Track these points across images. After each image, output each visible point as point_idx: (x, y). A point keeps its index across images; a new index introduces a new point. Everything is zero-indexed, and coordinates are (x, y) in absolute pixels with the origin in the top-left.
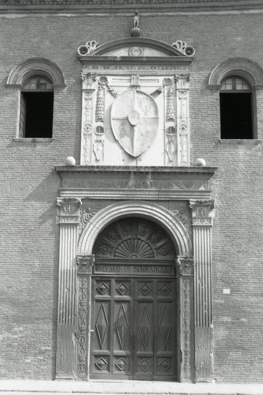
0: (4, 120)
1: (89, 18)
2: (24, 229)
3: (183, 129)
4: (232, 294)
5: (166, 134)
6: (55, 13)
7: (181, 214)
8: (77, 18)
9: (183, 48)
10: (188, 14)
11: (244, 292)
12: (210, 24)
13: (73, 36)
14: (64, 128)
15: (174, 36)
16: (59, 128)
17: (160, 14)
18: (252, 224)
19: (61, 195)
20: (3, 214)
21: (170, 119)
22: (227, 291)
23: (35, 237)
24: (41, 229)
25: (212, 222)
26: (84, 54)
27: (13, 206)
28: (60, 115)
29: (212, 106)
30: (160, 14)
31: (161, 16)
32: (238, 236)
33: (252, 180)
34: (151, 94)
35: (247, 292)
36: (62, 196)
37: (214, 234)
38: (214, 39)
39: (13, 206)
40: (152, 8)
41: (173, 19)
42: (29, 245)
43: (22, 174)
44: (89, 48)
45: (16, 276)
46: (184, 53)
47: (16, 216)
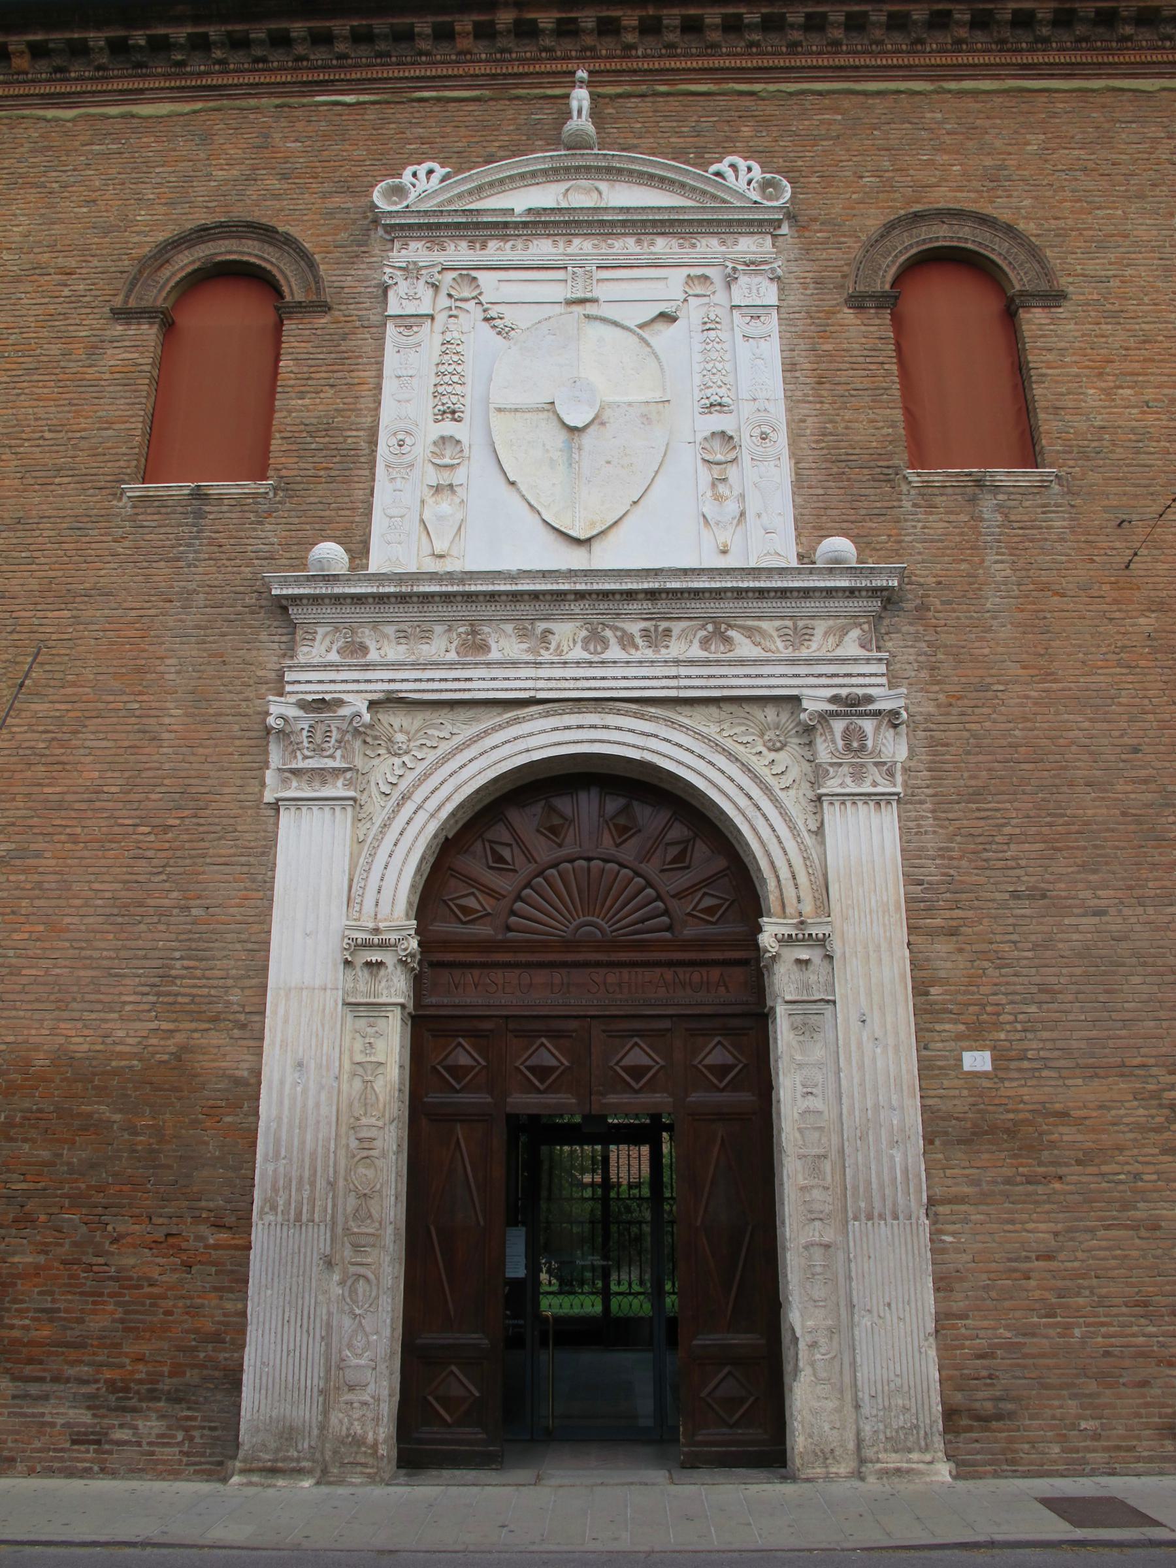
0: (97, 426)
1: (422, 104)
2: (137, 821)
3: (764, 437)
4: (1001, 1074)
5: (699, 457)
6: (303, 94)
7: (770, 750)
8: (377, 106)
9: (749, 183)
10: (757, 87)
11: (1051, 1064)
12: (839, 117)
13: (362, 158)
14: (313, 446)
15: (717, 150)
16: (294, 447)
17: (663, 88)
18: (1057, 781)
19: (288, 688)
20: (59, 767)
21: (712, 405)
22: (977, 1061)
23: (179, 853)
24: (202, 821)
25: (899, 779)
26: (395, 204)
27: (102, 736)
28: (300, 402)
29: (868, 360)
30: (663, 88)
31: (668, 94)
32: (1007, 830)
33: (1041, 615)
34: (641, 326)
35: (1062, 1063)
36: (289, 693)
37: (911, 824)
38: (855, 159)
39: (102, 736)
40: (635, 72)
41: (712, 104)
42: (151, 886)
43: (142, 612)
44: (414, 186)
45: (94, 1016)
46: (755, 196)
47: (109, 774)
